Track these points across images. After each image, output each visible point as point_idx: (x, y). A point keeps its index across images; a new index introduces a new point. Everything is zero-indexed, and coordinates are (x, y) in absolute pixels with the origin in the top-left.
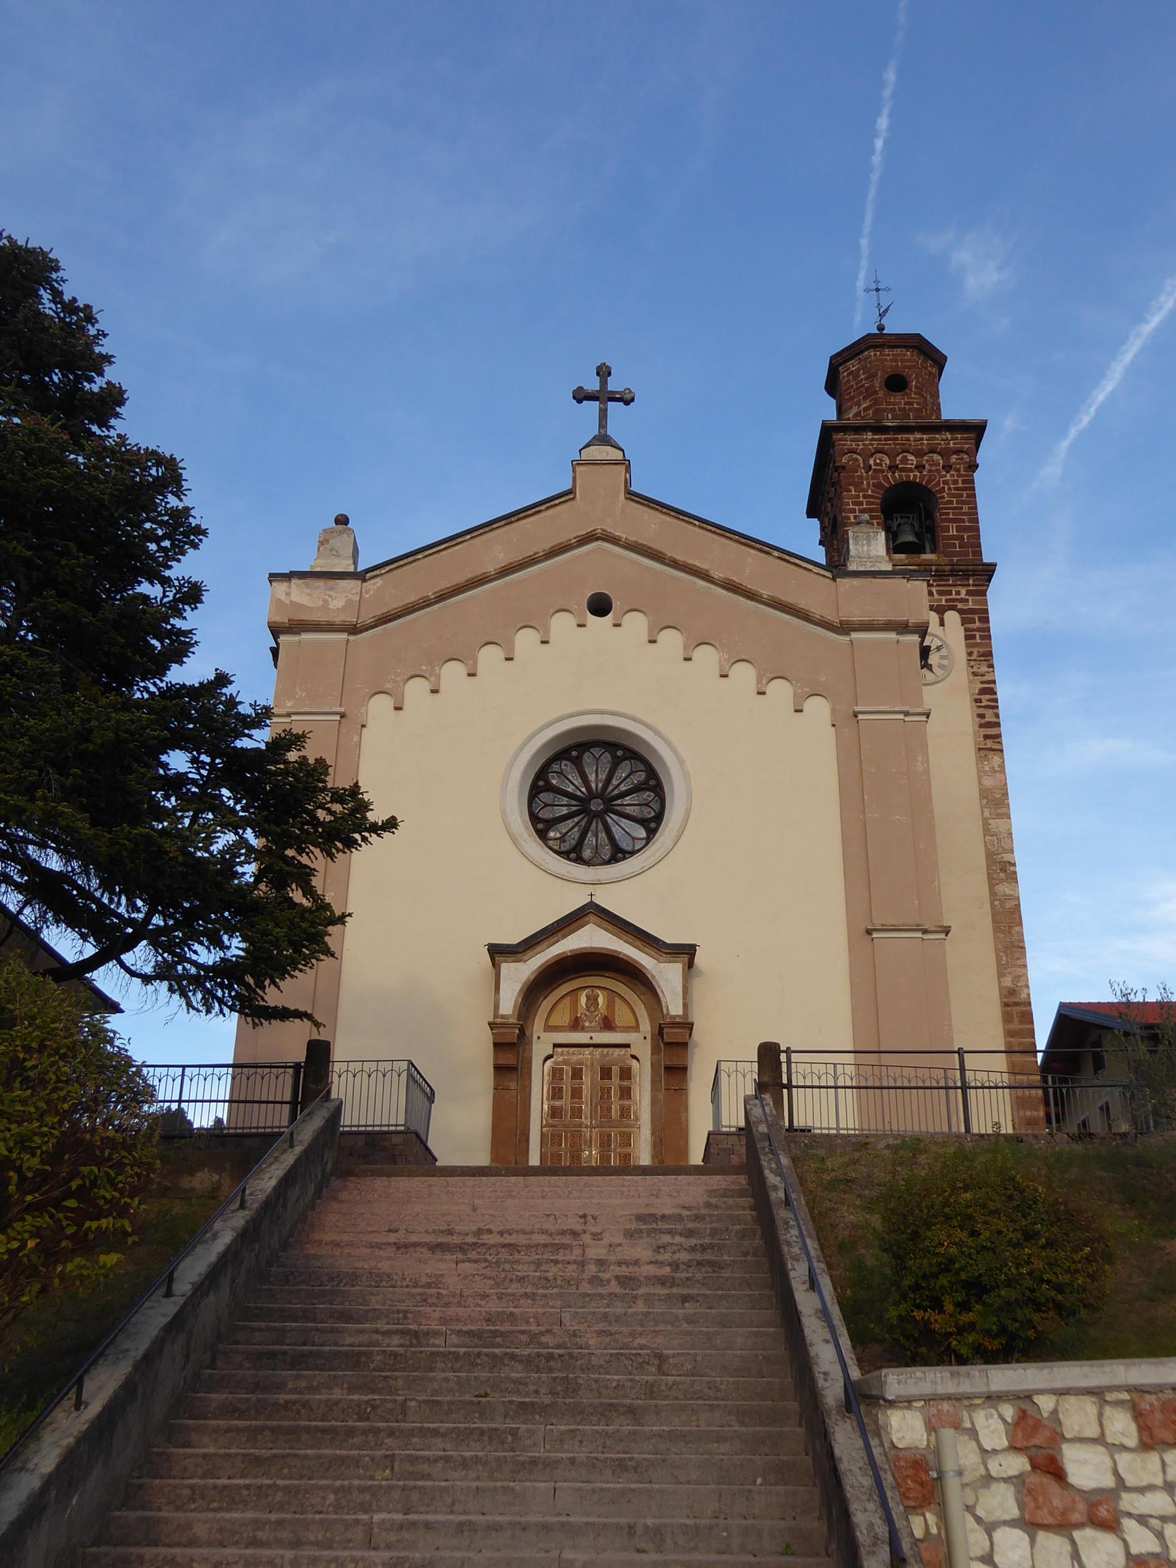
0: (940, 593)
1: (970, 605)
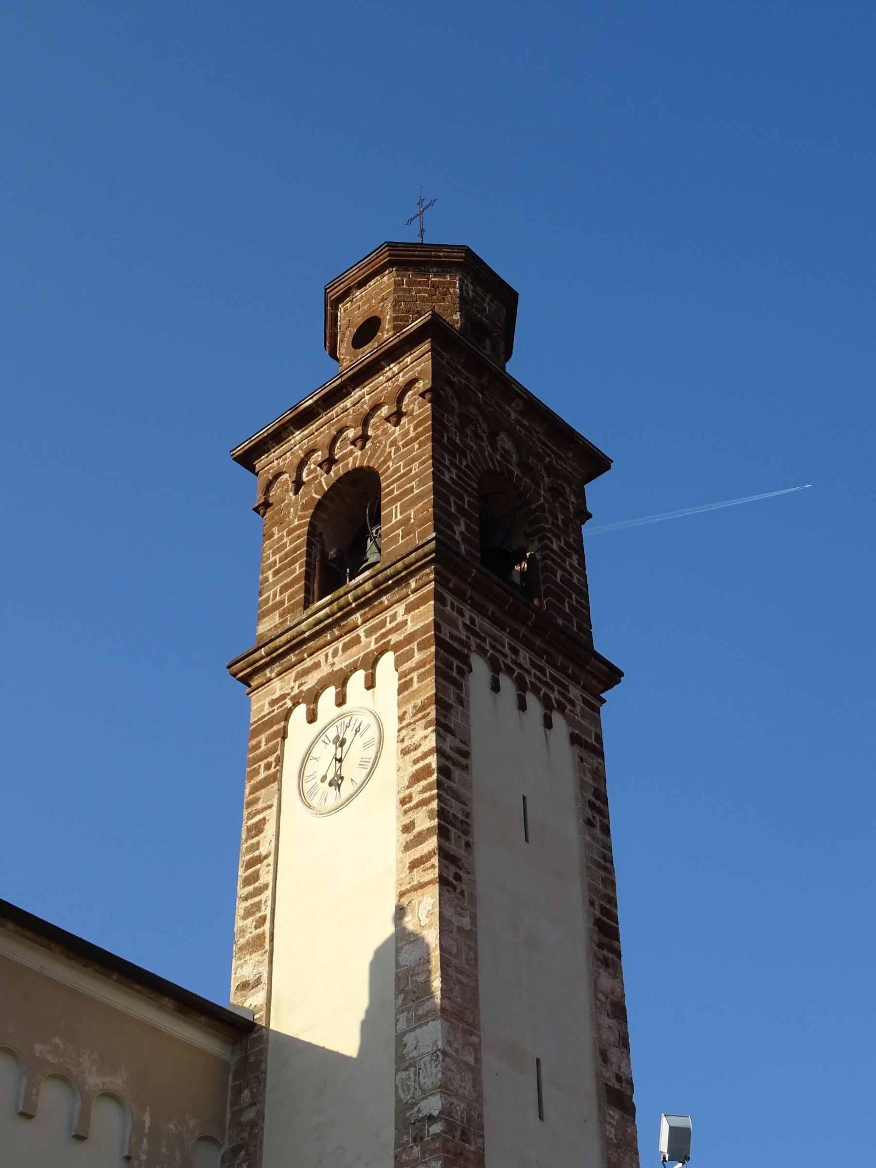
0: (368, 633)
1: (410, 628)
